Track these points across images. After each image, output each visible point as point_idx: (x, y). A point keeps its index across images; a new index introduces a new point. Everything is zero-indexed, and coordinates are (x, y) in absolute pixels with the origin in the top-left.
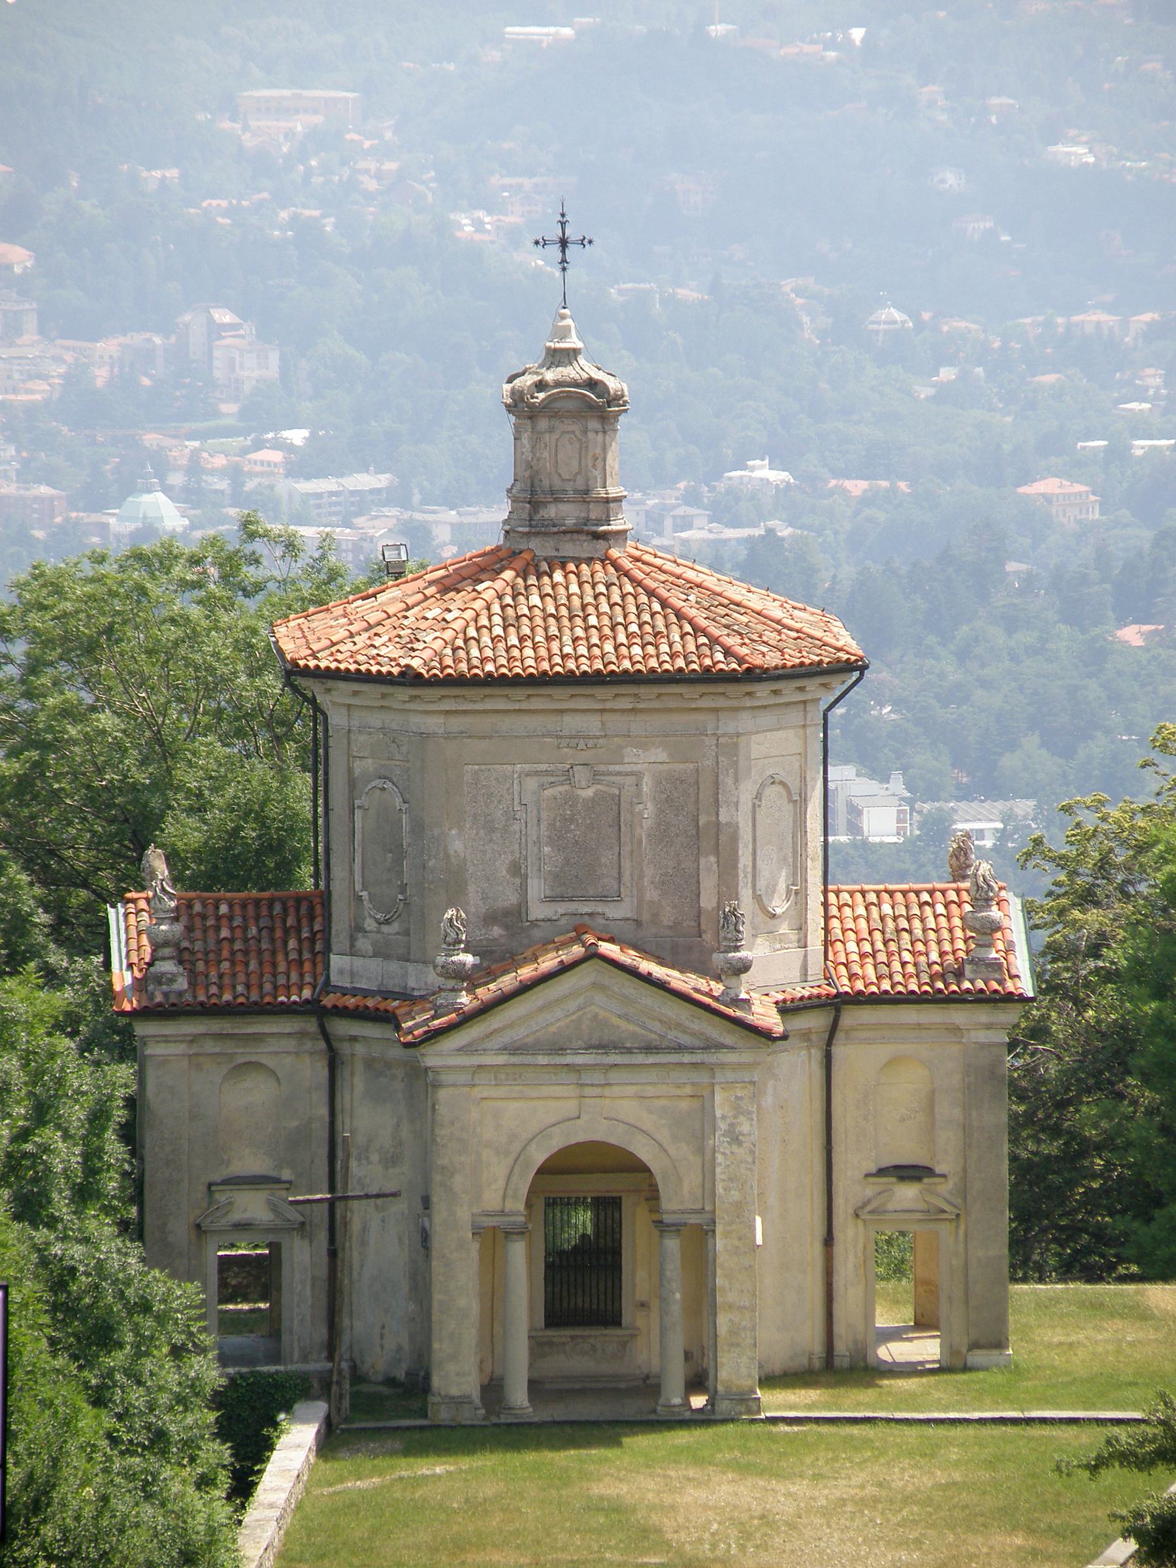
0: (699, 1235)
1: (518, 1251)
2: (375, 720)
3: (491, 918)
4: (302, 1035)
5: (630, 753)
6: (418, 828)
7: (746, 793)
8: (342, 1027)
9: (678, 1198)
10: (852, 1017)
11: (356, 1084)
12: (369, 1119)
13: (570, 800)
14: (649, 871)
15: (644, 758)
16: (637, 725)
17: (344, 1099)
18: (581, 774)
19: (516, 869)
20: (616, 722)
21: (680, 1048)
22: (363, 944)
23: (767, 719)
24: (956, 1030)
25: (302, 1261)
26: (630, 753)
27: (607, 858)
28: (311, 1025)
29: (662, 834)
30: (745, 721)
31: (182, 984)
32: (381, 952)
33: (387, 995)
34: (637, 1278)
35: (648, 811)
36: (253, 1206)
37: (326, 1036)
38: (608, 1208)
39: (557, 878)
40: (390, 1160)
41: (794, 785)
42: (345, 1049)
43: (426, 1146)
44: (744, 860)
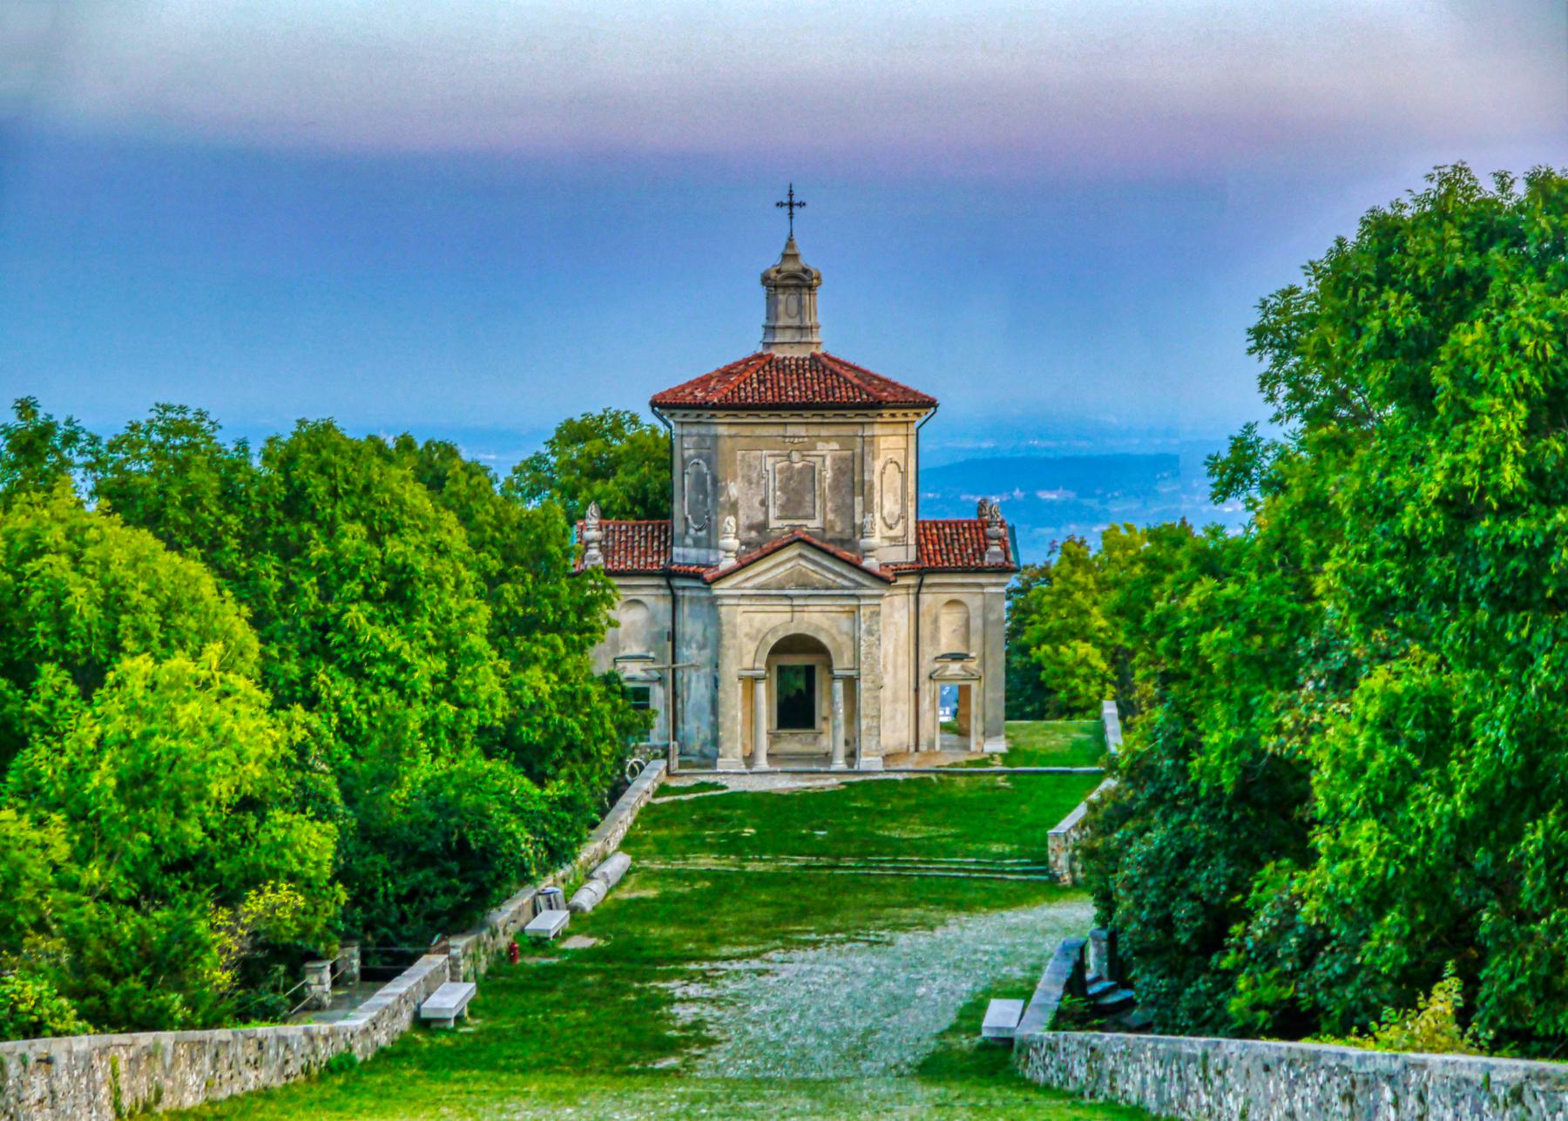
0: (851, 683)
1: (762, 688)
2: (694, 430)
3: (750, 528)
4: (659, 587)
5: (820, 445)
6: (715, 481)
7: (878, 465)
8: (678, 583)
9: (842, 665)
10: (928, 580)
11: (685, 610)
12: (691, 627)
13: (790, 468)
14: (829, 505)
15: (826, 450)
16: (824, 432)
17: (679, 619)
18: (795, 456)
19: (763, 503)
20: (813, 431)
21: (844, 588)
22: (689, 541)
23: (889, 430)
24: (980, 585)
25: (658, 696)
26: (820, 445)
27: (808, 498)
28: (663, 582)
29: (836, 486)
30: (877, 430)
31: (601, 560)
32: (697, 543)
33: (699, 565)
34: (821, 708)
35: (829, 474)
36: (634, 670)
37: (670, 587)
38: (810, 671)
39: (783, 507)
40: (702, 647)
41: (902, 464)
42: (680, 593)
43: (719, 638)
44: (877, 500)
